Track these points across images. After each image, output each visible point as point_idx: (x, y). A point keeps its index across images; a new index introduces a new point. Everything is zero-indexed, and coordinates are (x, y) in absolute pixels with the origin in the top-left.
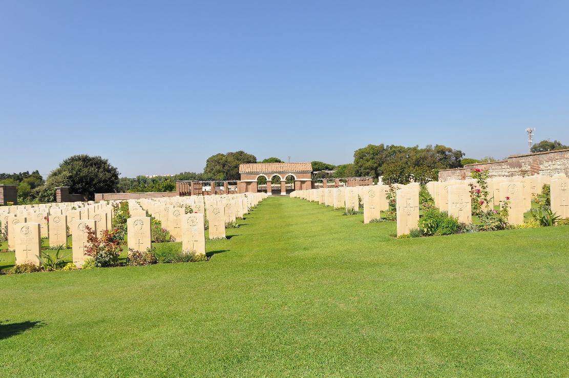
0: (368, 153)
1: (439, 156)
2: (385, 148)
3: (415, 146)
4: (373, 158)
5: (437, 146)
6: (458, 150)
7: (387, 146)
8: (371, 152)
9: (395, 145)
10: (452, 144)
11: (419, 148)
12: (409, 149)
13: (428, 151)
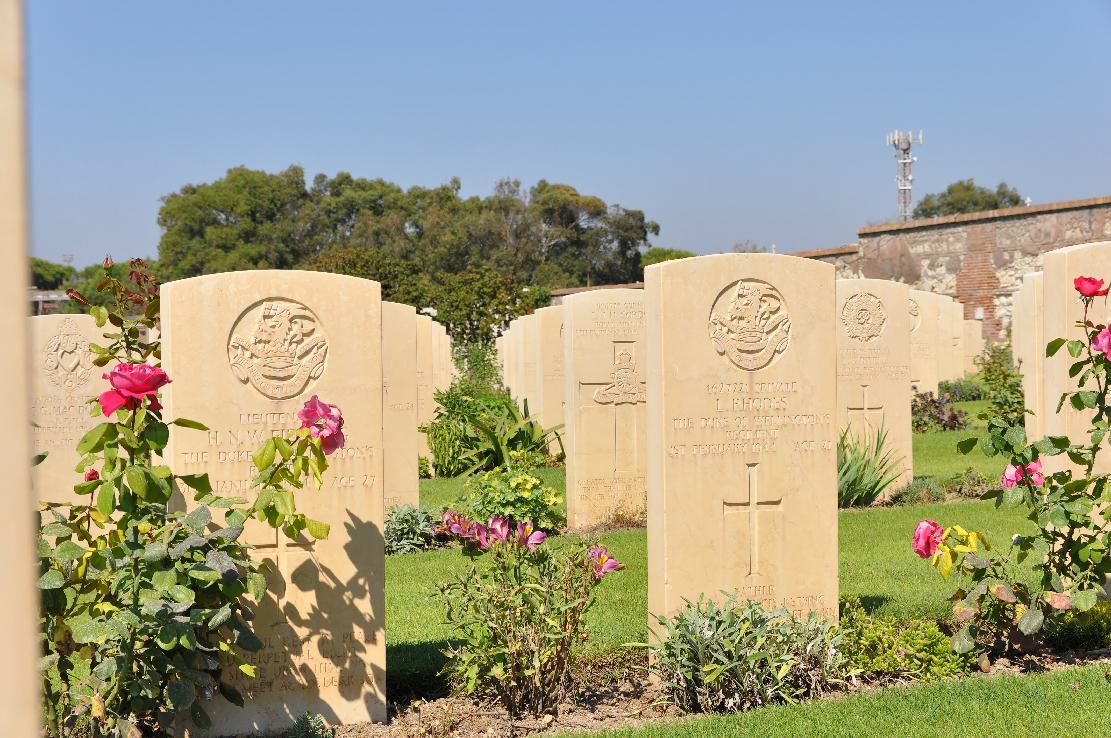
0: (228, 209)
1: (548, 233)
2: (309, 186)
3: (447, 182)
4: (248, 236)
5: (543, 186)
6: (632, 207)
7: (320, 178)
8: (243, 207)
9: (355, 177)
11: (464, 195)
12: (419, 195)
13: (503, 206)
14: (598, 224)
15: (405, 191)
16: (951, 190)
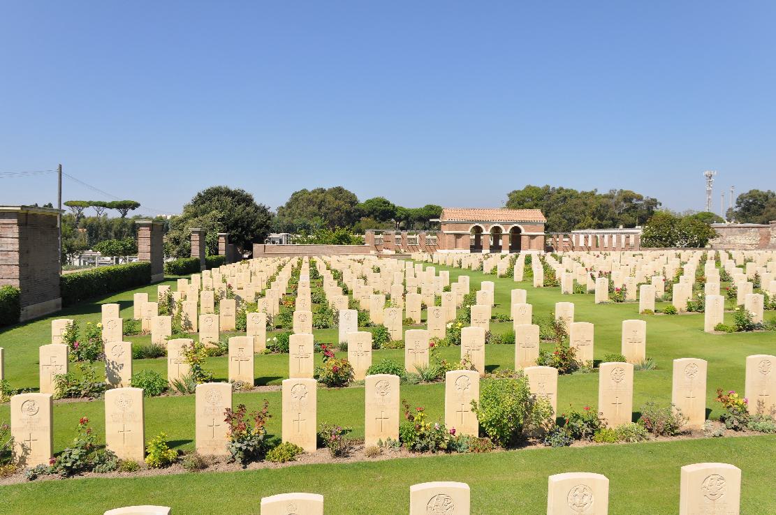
0: (532, 198)
5: (622, 191)
10: (644, 190)
11: (597, 194)
12: (584, 193)
13: (611, 197)
15: (580, 192)
16: (750, 192)
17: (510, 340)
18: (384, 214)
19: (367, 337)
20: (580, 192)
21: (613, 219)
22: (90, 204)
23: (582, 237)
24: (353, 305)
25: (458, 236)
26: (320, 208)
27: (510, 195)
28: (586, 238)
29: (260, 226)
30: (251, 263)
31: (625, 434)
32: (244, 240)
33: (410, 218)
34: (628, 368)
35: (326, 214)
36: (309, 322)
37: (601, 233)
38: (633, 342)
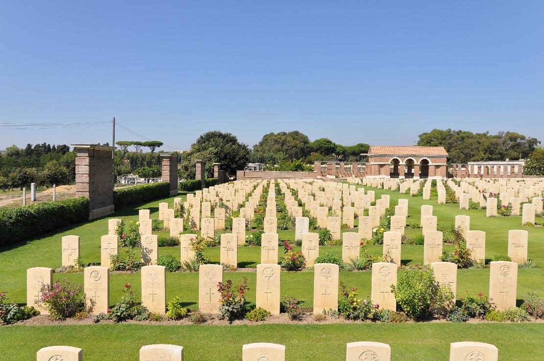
3: (485, 132)
5: (508, 133)
6: (533, 137)
7: (454, 131)
11: (488, 135)
13: (500, 137)
14: (524, 141)
15: (474, 134)
17: (421, 242)
18: (327, 150)
19: (316, 236)
20: (474, 134)
21: (501, 154)
22: (131, 143)
23: (476, 167)
24: (305, 214)
25: (381, 166)
26: (282, 146)
27: (420, 136)
28: (479, 168)
29: (240, 159)
30: (235, 183)
31: (510, 316)
32: (231, 168)
33: (346, 153)
34: (513, 266)
35: (287, 150)
36: (275, 225)
37: (491, 164)
38: (517, 246)
